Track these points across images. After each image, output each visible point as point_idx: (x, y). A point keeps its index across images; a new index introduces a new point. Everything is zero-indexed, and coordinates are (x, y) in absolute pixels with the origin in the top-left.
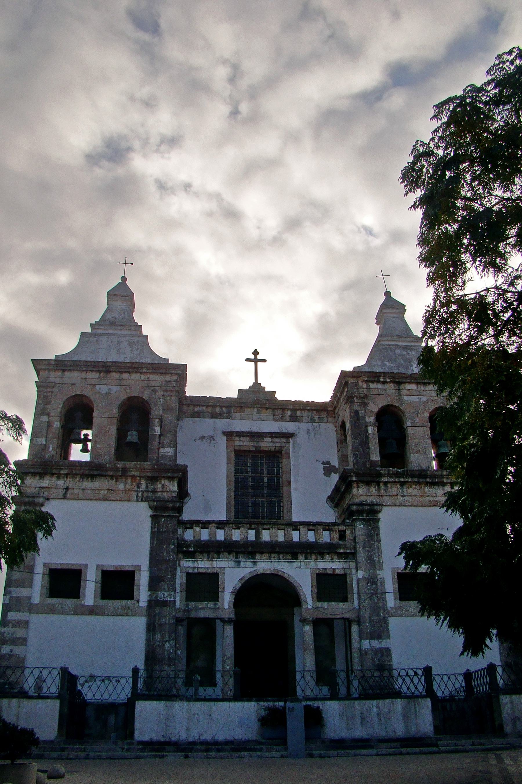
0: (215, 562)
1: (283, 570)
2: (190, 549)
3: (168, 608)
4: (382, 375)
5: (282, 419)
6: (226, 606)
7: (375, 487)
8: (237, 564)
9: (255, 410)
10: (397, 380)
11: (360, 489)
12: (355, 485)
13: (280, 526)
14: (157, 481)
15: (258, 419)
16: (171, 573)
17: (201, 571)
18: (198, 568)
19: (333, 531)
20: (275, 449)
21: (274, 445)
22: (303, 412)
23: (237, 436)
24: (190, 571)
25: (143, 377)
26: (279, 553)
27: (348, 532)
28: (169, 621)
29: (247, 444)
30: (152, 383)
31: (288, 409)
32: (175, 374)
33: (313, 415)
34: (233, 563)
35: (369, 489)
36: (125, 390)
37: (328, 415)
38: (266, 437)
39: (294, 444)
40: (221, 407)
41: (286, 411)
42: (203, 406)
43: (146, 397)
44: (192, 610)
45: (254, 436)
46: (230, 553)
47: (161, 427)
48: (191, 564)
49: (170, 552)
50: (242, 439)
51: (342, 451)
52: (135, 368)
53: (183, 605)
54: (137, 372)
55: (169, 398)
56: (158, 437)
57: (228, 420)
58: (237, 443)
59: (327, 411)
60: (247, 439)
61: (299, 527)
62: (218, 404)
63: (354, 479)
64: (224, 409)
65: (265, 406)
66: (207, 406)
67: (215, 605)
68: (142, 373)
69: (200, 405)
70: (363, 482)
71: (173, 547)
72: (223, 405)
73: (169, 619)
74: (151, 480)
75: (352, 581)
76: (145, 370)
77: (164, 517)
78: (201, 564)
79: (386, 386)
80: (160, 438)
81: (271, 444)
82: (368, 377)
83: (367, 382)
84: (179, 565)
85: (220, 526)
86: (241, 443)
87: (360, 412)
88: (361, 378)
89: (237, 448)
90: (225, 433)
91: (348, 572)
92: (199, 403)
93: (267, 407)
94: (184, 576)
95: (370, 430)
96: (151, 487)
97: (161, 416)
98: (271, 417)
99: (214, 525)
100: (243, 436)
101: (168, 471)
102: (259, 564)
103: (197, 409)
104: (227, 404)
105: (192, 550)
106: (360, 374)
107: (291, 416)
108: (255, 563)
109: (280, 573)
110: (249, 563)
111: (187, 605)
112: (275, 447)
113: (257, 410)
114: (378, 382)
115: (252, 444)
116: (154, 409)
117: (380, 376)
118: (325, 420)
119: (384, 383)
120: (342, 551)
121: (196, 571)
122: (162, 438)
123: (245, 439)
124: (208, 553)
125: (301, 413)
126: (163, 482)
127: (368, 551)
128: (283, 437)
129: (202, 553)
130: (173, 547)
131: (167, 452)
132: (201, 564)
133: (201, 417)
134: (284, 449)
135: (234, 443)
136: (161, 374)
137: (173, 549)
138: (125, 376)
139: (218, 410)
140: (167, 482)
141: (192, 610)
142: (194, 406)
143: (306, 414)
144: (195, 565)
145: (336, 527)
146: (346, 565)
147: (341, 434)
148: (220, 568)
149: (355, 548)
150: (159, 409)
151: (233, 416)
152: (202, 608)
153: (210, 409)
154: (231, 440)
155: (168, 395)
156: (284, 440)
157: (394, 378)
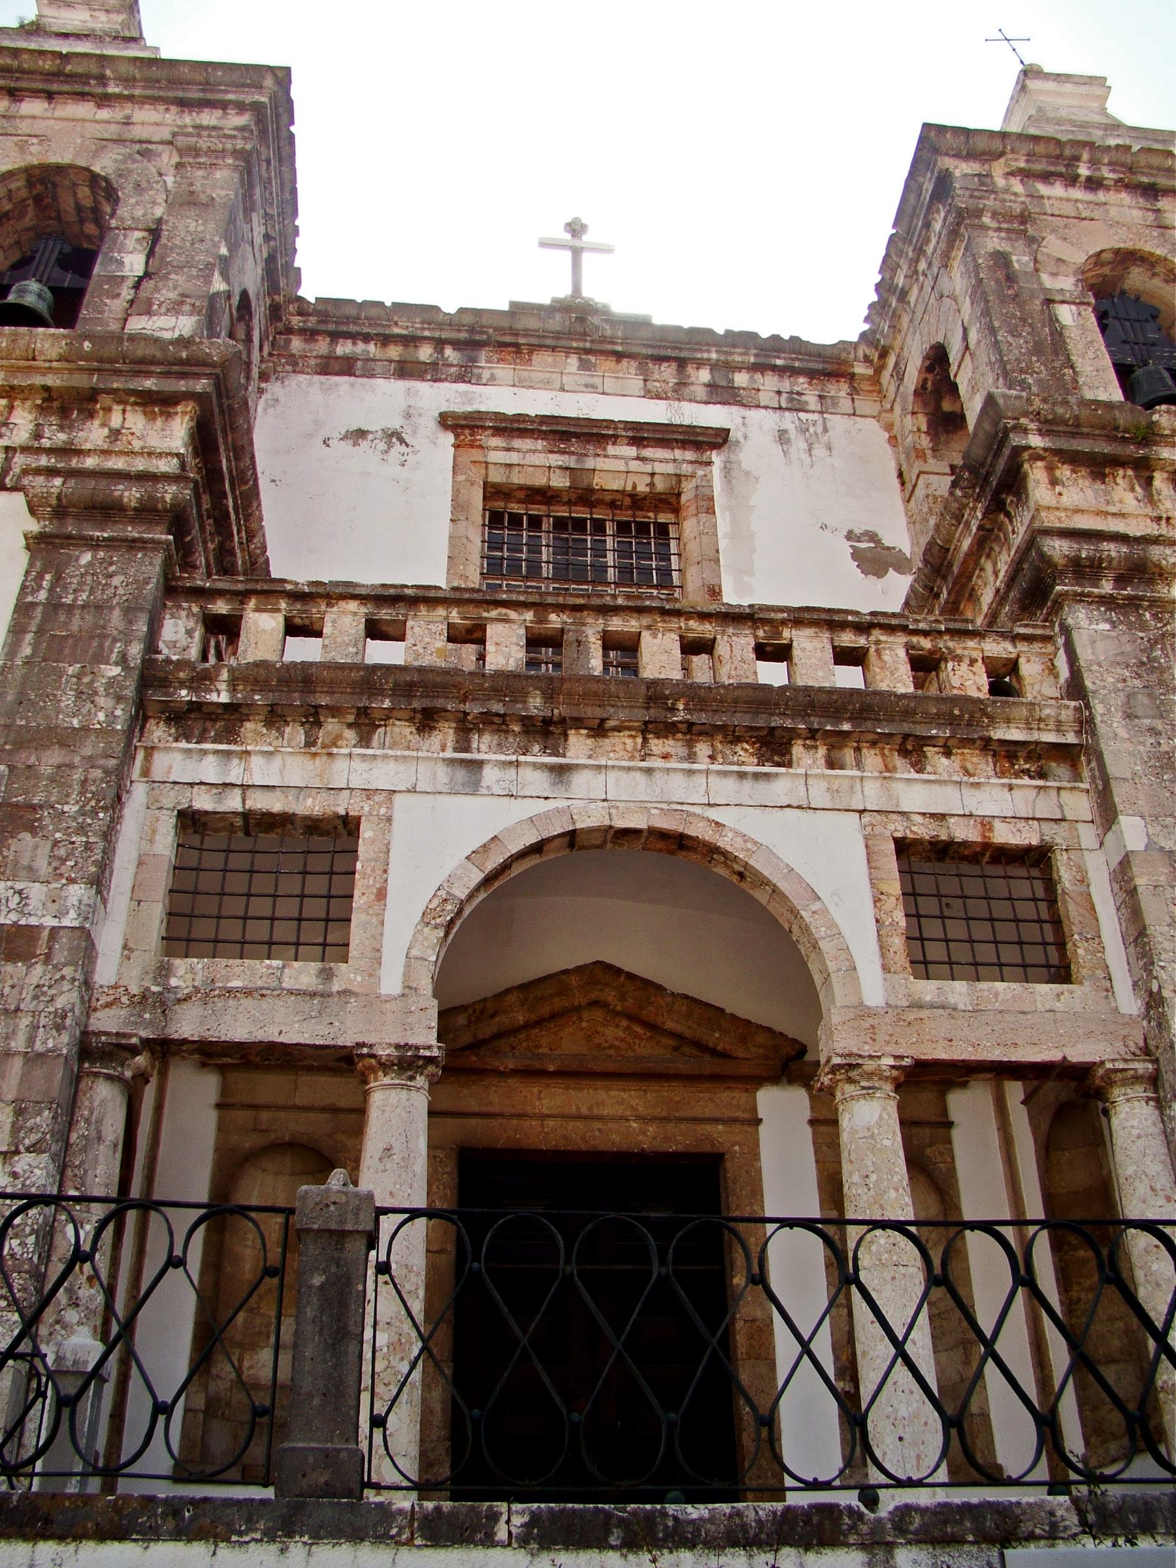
0: (341, 765)
1: (712, 814)
2: (213, 697)
3: (39, 969)
4: (1085, 156)
5: (680, 391)
6: (391, 983)
7: (1132, 490)
8: (461, 774)
9: (573, 361)
10: (1145, 179)
11: (1064, 491)
12: (1036, 474)
13: (692, 623)
14: (91, 415)
15: (584, 389)
16: (82, 793)
17: (260, 802)
18: (245, 787)
19: (958, 659)
20: (652, 485)
21: (648, 468)
22: (758, 376)
23: (498, 431)
24: (204, 802)
25: (104, 114)
26: (691, 732)
27: (1030, 669)
28: (31, 1040)
29: (540, 459)
30: (137, 132)
31: (700, 364)
32: (241, 107)
33: (797, 389)
34: (443, 774)
35: (1106, 493)
36: (22, 148)
37: (854, 392)
38: (614, 439)
39: (727, 469)
40: (440, 344)
41: (690, 369)
42: (366, 338)
43: (103, 168)
44: (187, 998)
45: (565, 436)
46: (426, 721)
47: (150, 254)
48: (210, 769)
49: (96, 693)
50: (517, 443)
51: (928, 486)
52: (72, 77)
53: (136, 972)
54: (82, 96)
55: (201, 173)
56: (130, 283)
57: (462, 387)
58: (496, 457)
59: (852, 377)
60: (540, 444)
61: (786, 633)
62: (427, 333)
63: (1036, 441)
64: (449, 352)
65: (610, 347)
66: (386, 340)
67: (327, 975)
68: (104, 100)
69: (353, 337)
70: (1074, 459)
71: (116, 671)
72: (445, 335)
73: (35, 1027)
74: (64, 412)
75: (1083, 881)
76: (113, 89)
77: (94, 544)
78: (260, 771)
79: (1101, 196)
80: (137, 286)
81: (635, 465)
82: (1030, 156)
83: (1025, 175)
84: (146, 772)
85: (385, 614)
86: (514, 458)
87: (1014, 258)
88: (1002, 160)
89: (496, 477)
90: (448, 422)
91: (1058, 836)
92: (353, 328)
93: (619, 348)
94: (167, 825)
95: (1065, 314)
96: (55, 436)
97: (159, 221)
98: (636, 384)
99: (353, 605)
100: (523, 433)
101: (141, 366)
102: (581, 782)
103: (344, 348)
104: (463, 335)
105: (224, 698)
106: (997, 145)
107: (712, 386)
108: (561, 772)
109: (696, 830)
110: (528, 774)
111: (163, 972)
112: (653, 474)
113: (580, 360)
114: (1072, 180)
115: (556, 460)
116: (133, 201)
117: (1077, 158)
118: (845, 404)
119: (1094, 184)
120: (1015, 734)
121: (233, 803)
122: (148, 285)
123: (527, 444)
124: (313, 718)
125: (752, 379)
126: (116, 420)
127: (1153, 731)
128: (684, 444)
129: (275, 718)
130: (116, 671)
131: (161, 329)
132: (260, 771)
133: (358, 373)
134: (688, 489)
135: (486, 456)
136: (184, 104)
137: (111, 682)
138: (33, 107)
139: (425, 353)
140: (136, 421)
141: (187, 998)
142: (335, 336)
143: (769, 383)
144: (235, 773)
145: (971, 644)
146: (1045, 806)
147: (919, 430)
148: (369, 793)
149: (1086, 723)
150: (154, 203)
151: (486, 375)
152: (248, 992)
153: (394, 352)
154: (472, 446)
155: (200, 166)
156: (690, 455)
157: (1131, 169)
